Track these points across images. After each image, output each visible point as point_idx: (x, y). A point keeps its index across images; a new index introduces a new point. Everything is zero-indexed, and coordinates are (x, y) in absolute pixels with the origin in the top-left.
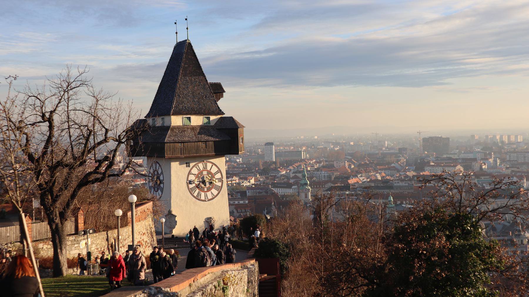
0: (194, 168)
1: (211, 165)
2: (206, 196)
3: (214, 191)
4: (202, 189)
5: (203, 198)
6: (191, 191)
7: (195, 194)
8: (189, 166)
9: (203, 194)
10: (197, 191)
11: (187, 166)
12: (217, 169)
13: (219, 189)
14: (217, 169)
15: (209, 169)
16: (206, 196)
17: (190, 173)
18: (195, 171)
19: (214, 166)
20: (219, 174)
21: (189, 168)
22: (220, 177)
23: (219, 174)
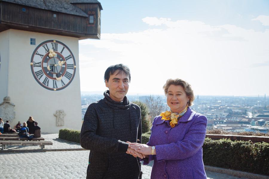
0: (41, 47)
1: (62, 46)
2: (55, 84)
3: (66, 81)
4: (50, 75)
5: (51, 85)
6: (36, 76)
7: (42, 81)
8: (34, 44)
9: (51, 81)
10: (44, 76)
11: (31, 43)
12: (69, 54)
13: (71, 77)
14: (69, 54)
15: (59, 51)
16: (55, 84)
17: (35, 52)
18: (42, 51)
19: (66, 49)
20: (72, 59)
21: (34, 47)
22: (72, 63)
23: (72, 59)
